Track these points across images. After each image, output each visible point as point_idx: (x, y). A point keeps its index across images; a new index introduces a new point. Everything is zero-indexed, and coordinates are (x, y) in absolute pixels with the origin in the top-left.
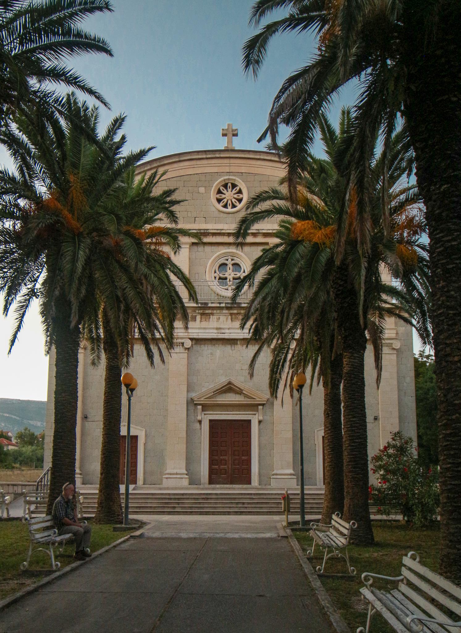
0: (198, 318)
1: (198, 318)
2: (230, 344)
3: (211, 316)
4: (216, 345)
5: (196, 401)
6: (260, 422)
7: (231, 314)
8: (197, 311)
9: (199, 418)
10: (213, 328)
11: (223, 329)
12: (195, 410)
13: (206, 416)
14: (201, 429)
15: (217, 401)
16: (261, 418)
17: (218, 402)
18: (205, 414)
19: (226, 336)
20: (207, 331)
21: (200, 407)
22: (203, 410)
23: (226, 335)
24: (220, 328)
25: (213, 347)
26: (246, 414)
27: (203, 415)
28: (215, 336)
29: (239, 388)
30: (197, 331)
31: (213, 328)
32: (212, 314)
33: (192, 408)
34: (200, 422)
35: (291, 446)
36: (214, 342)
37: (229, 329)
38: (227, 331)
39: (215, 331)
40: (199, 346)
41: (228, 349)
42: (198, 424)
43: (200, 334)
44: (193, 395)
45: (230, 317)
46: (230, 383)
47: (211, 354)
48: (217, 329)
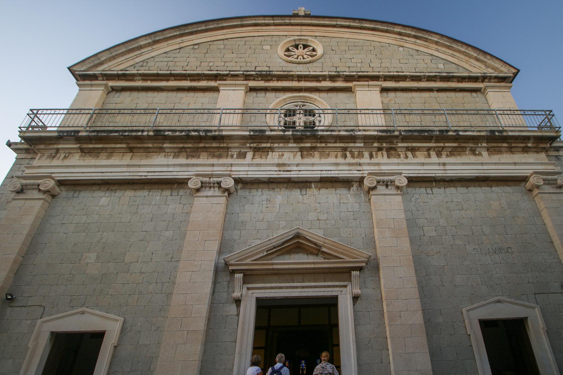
0: (250, 155)
1: (250, 155)
2: (300, 188)
3: (270, 153)
4: (276, 190)
5: (232, 265)
6: (355, 298)
7: (302, 149)
8: (248, 145)
9: (237, 294)
10: (272, 165)
11: (288, 165)
12: (231, 282)
13: (251, 292)
14: (238, 315)
15: (273, 264)
16: (357, 291)
17: (275, 267)
18: (248, 289)
19: (293, 175)
20: (262, 168)
21: (239, 276)
22: (245, 281)
23: (292, 173)
24: (284, 165)
25: (271, 192)
26: (329, 287)
27: (245, 290)
28: (275, 175)
29: (315, 244)
30: (246, 168)
31: (272, 165)
32: (272, 149)
33: (224, 279)
34: (238, 302)
35: (425, 341)
36: (272, 186)
37: (297, 165)
38: (295, 168)
39: (275, 168)
40: (247, 191)
41: (296, 194)
42: (234, 307)
43: (249, 173)
44: (231, 257)
45: (299, 153)
46: (298, 236)
47: (267, 200)
48: (278, 165)
